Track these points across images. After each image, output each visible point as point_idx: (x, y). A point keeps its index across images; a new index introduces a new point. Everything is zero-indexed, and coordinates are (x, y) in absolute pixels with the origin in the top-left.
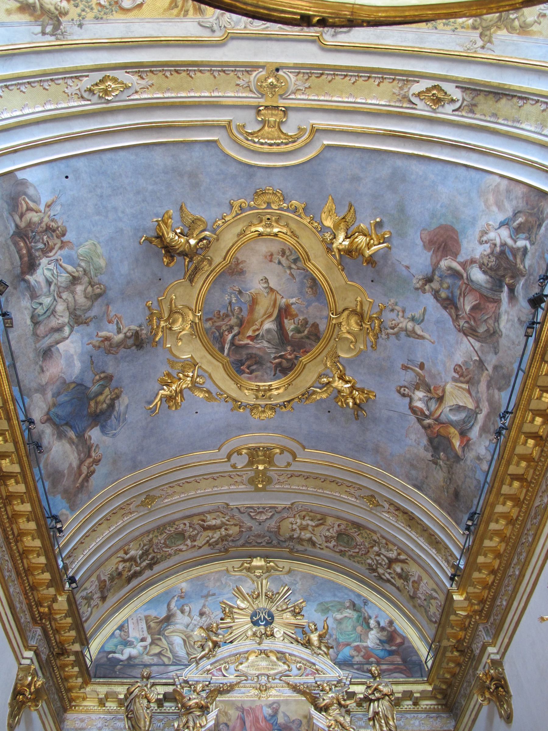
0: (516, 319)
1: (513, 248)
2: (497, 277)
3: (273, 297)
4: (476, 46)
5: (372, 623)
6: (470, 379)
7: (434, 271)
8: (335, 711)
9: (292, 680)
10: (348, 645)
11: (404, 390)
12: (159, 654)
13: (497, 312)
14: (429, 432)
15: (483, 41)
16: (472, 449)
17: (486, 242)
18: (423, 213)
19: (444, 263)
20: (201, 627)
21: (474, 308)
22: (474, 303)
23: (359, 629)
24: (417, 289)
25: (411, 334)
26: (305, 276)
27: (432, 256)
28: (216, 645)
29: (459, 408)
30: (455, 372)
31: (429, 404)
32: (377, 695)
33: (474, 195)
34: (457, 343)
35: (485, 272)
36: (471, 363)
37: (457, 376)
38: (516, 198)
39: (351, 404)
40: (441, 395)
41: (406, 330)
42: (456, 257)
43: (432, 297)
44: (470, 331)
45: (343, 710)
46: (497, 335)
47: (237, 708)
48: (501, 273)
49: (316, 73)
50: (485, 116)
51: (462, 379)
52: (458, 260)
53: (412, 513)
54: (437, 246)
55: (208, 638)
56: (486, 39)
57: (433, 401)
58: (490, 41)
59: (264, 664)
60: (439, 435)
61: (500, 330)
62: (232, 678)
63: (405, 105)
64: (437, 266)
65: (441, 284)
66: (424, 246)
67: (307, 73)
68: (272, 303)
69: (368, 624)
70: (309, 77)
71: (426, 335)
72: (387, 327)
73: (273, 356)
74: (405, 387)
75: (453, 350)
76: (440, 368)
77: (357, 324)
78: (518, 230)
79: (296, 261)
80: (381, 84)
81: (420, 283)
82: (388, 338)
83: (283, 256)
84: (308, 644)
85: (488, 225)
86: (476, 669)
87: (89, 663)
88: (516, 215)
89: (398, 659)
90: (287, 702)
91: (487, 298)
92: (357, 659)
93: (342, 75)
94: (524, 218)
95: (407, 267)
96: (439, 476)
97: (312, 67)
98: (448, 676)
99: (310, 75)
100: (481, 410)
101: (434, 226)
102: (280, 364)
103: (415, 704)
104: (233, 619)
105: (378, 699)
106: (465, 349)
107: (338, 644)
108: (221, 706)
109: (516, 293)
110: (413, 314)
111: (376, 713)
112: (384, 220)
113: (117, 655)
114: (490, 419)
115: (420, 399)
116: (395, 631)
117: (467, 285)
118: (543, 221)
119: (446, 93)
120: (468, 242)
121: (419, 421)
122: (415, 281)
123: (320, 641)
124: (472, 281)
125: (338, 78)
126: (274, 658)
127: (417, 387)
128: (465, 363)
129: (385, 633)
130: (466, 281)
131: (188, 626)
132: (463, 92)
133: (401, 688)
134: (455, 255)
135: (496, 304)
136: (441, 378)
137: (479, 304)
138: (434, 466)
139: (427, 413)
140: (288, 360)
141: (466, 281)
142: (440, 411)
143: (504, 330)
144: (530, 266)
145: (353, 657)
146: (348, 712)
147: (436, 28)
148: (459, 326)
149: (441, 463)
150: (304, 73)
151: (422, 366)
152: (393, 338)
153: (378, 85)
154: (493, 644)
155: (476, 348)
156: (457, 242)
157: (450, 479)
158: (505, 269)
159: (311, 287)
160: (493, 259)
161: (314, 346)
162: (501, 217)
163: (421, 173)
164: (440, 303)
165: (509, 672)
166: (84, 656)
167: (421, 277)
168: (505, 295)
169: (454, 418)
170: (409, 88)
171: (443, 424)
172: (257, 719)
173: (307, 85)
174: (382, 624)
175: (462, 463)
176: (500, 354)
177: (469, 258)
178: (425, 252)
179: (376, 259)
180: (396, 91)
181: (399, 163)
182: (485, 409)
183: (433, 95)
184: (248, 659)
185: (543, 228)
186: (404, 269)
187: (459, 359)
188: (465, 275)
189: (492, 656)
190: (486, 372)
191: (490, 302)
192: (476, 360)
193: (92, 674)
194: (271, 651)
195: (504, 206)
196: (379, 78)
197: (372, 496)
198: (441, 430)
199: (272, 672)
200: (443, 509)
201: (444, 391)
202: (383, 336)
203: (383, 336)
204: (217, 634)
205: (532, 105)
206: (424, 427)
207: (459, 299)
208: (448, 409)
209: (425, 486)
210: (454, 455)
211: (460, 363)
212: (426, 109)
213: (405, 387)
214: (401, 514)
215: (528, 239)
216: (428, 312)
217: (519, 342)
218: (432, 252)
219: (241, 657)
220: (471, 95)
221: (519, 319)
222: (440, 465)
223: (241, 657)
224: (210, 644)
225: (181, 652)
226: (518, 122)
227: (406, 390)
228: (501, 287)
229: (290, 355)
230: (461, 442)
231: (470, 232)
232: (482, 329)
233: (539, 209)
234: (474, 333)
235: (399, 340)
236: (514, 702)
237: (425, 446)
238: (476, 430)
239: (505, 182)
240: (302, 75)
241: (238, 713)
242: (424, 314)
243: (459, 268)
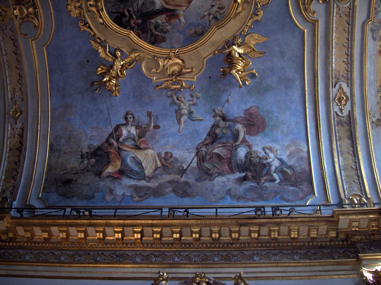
0: (228, 188)
1: (271, 171)
2: (248, 166)
3: (183, 4)
4: (373, 118)
6: (167, 166)
7: (232, 120)
11: (131, 118)
13: (225, 173)
14: (106, 145)
15: (376, 122)
16: (114, 184)
17: (265, 153)
18: (269, 104)
19: (239, 127)
21: (218, 156)
22: (222, 154)
24: (214, 111)
25: (179, 114)
26: (204, 27)
27: (241, 117)
29: (139, 164)
30: (165, 153)
31: (129, 140)
33: (291, 137)
34: (188, 149)
35: (246, 157)
36: (179, 164)
37: (163, 155)
38: (300, 165)
39: (105, 79)
40: (141, 147)
41: (180, 109)
42: (247, 134)
43: (213, 124)
44: (201, 157)
46: (209, 177)
48: (252, 169)
49: (349, 20)
50: (338, 133)
51: (163, 160)
52: (246, 136)
53: (26, 149)
54: (249, 119)
56: (377, 123)
57: (133, 142)
58: (377, 126)
60: (108, 154)
61: (214, 178)
63: (334, 80)
64: (236, 122)
65: (224, 128)
66: (247, 110)
67: (349, 15)
68: (178, 3)
70: (347, 16)
71: (182, 125)
72: (177, 94)
73: (131, 9)
74: (134, 118)
75: (181, 148)
76: (163, 141)
77: (173, 72)
78: (283, 172)
79: (215, 18)
80: (344, 63)
81: (220, 112)
82: (169, 97)
83: (218, 8)
85: (276, 151)
88: (290, 167)
91: (231, 163)
93: (349, 37)
94: (291, 174)
95: (228, 101)
96: (74, 163)
97: (353, 17)
99: (348, 16)
100: (149, 182)
101: (262, 114)
102: (125, 16)
106: (186, 156)
109: (244, 182)
110: (194, 112)
112: (257, 78)
114: (147, 190)
115: (129, 132)
117: (232, 146)
118: (296, 187)
119: (345, 105)
120: (260, 140)
121: (111, 135)
122: (219, 108)
124: (236, 149)
125: (347, 35)
127: (137, 127)
128: (177, 160)
130: (234, 145)
132: (347, 115)
134: (248, 133)
135: (229, 170)
136: (154, 144)
137: (224, 158)
138: (80, 157)
139: (121, 140)
140: (129, 21)
141: (234, 145)
142: (128, 150)
143: (215, 181)
144: (266, 187)
147: (378, 92)
148: (201, 148)
149: (86, 162)
150: (350, 12)
151: (157, 127)
152: (170, 100)
153: (344, 61)
155: (191, 165)
156: (256, 133)
157: (77, 173)
158: (255, 170)
159: (195, 33)
160: (257, 160)
161: (145, 41)
162: (284, 158)
163: (294, 98)
164: (210, 130)
167: (224, 112)
168: (238, 175)
169: (129, 161)
170: (343, 81)
171: (119, 155)
173: (342, 15)
175: (97, 178)
176: (199, 184)
177: (251, 143)
178: (243, 112)
179: (227, 77)
180: (341, 73)
181: (298, 82)
182: (153, 184)
183: (343, 98)
185: (292, 188)
186: (226, 99)
187: (177, 154)
188: (238, 143)
190: (179, 177)
191: (229, 166)
192: (183, 167)
195: (292, 159)
196: (348, 61)
197: (21, 112)
198: (113, 155)
200: (47, 174)
201: (145, 149)
202: (169, 93)
203: (169, 93)
205: (353, 160)
206: (107, 141)
207: (220, 143)
208: (133, 156)
209: (56, 153)
210: (99, 170)
211: (174, 155)
212: (334, 94)
213: (134, 118)
214: (18, 140)
215: (281, 180)
216: (200, 122)
217: (215, 195)
218: (244, 116)
220: (347, 121)
221: (229, 190)
222: (83, 162)
226: (341, 154)
227: (132, 119)
228: (243, 170)
229: (134, 23)
230: (114, 173)
231: (267, 139)
232: (206, 165)
233: (301, 182)
234: (201, 161)
235: (170, 105)
237: (92, 145)
238: (133, 182)
239: (306, 155)
240: (348, 11)
242: (198, 120)
243: (241, 138)
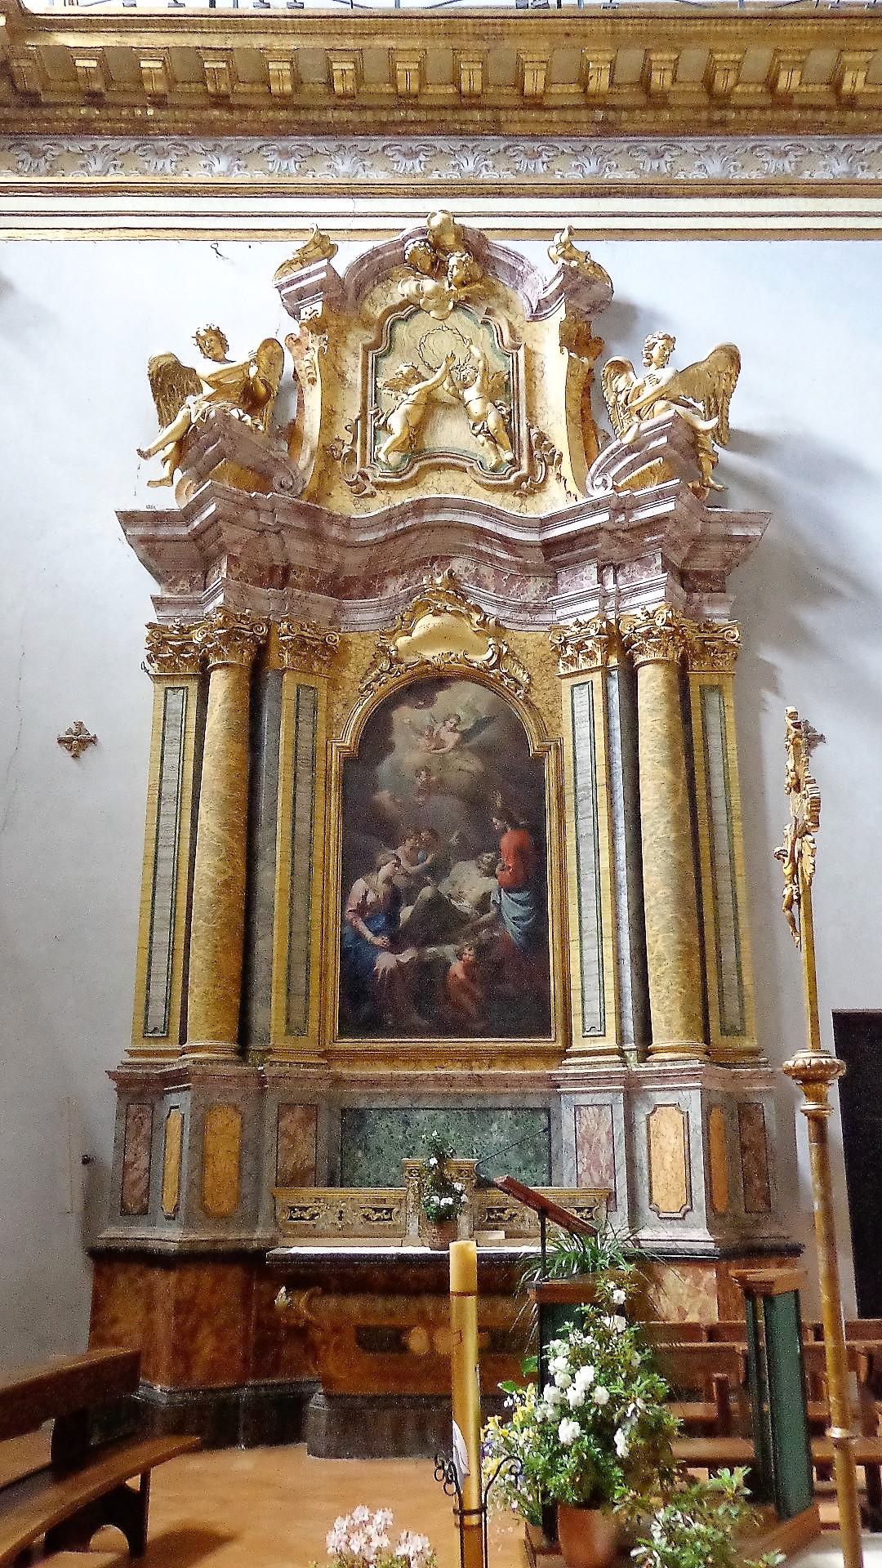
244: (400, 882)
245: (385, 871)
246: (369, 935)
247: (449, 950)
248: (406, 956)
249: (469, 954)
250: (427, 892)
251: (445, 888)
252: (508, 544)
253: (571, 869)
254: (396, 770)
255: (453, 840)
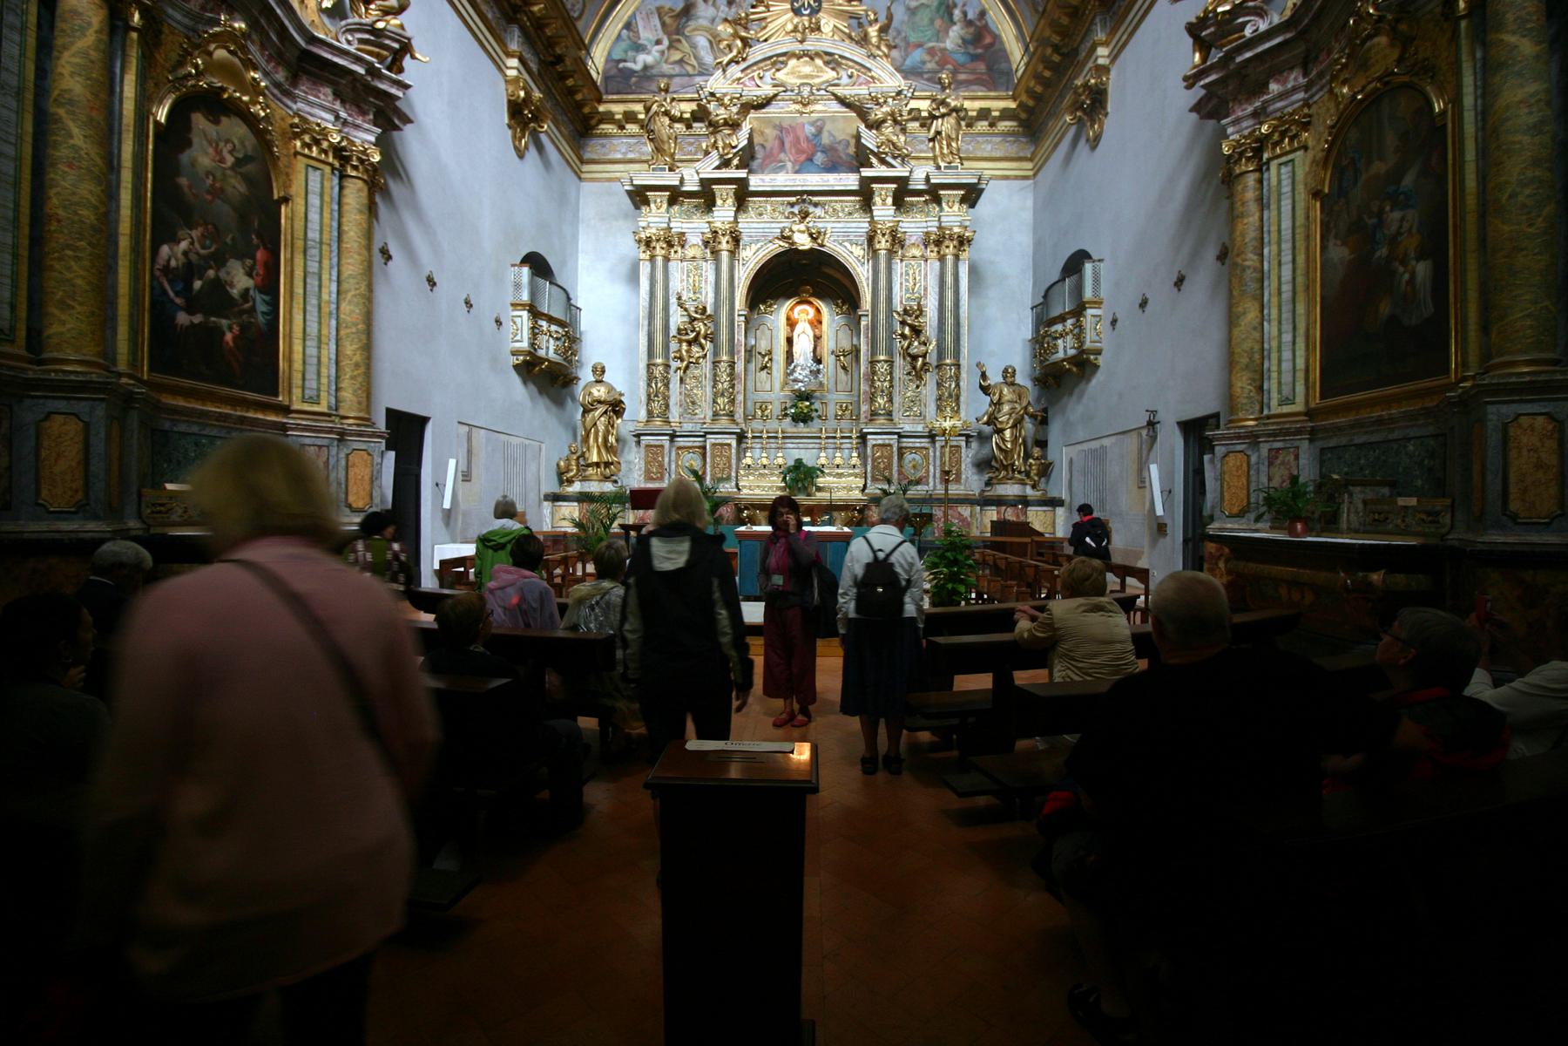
5: (957, 13)
8: (888, 129)
9: (839, 91)
10: (920, 45)
12: (681, 62)
20: (726, 20)
23: (938, 23)
28: (746, 43)
32: (943, 110)
45: (898, 128)
47: (775, 127)
55: (736, 35)
59: (807, 69)
62: (767, 90)
69: (951, 15)
84: (863, 41)
86: (1076, 77)
87: (594, 75)
89: (982, 67)
90: (833, 119)
92: (930, 66)
98: (1039, 89)
103: (992, 125)
104: (767, 7)
105: (943, 116)
107: (908, 44)
108: (756, 125)
111: (938, 133)
113: (630, 65)
116: (986, 27)
123: (880, 39)
126: (819, 62)
129: (972, 30)
131: (713, 21)
133: (978, 104)
145: (924, 63)
146: (904, 130)
154: (1105, 44)
165: (1114, 84)
166: (585, 65)
172: (797, 140)
174: (970, 16)
184: (785, 63)
189: (1101, 61)
193: (602, 90)
194: (817, 54)
199: (817, 81)
204: (746, 29)
219: (778, 61)
223: (778, 61)
224: (739, 43)
225: (709, 59)
236: (1109, 123)
241: (776, 132)
244: (193, 257)
245: (184, 245)
246: (171, 294)
247: (224, 322)
248: (198, 319)
249: (236, 329)
250: (211, 273)
251: (222, 275)
252: (283, 32)
253: (299, 290)
254: (193, 163)
255: (228, 240)
